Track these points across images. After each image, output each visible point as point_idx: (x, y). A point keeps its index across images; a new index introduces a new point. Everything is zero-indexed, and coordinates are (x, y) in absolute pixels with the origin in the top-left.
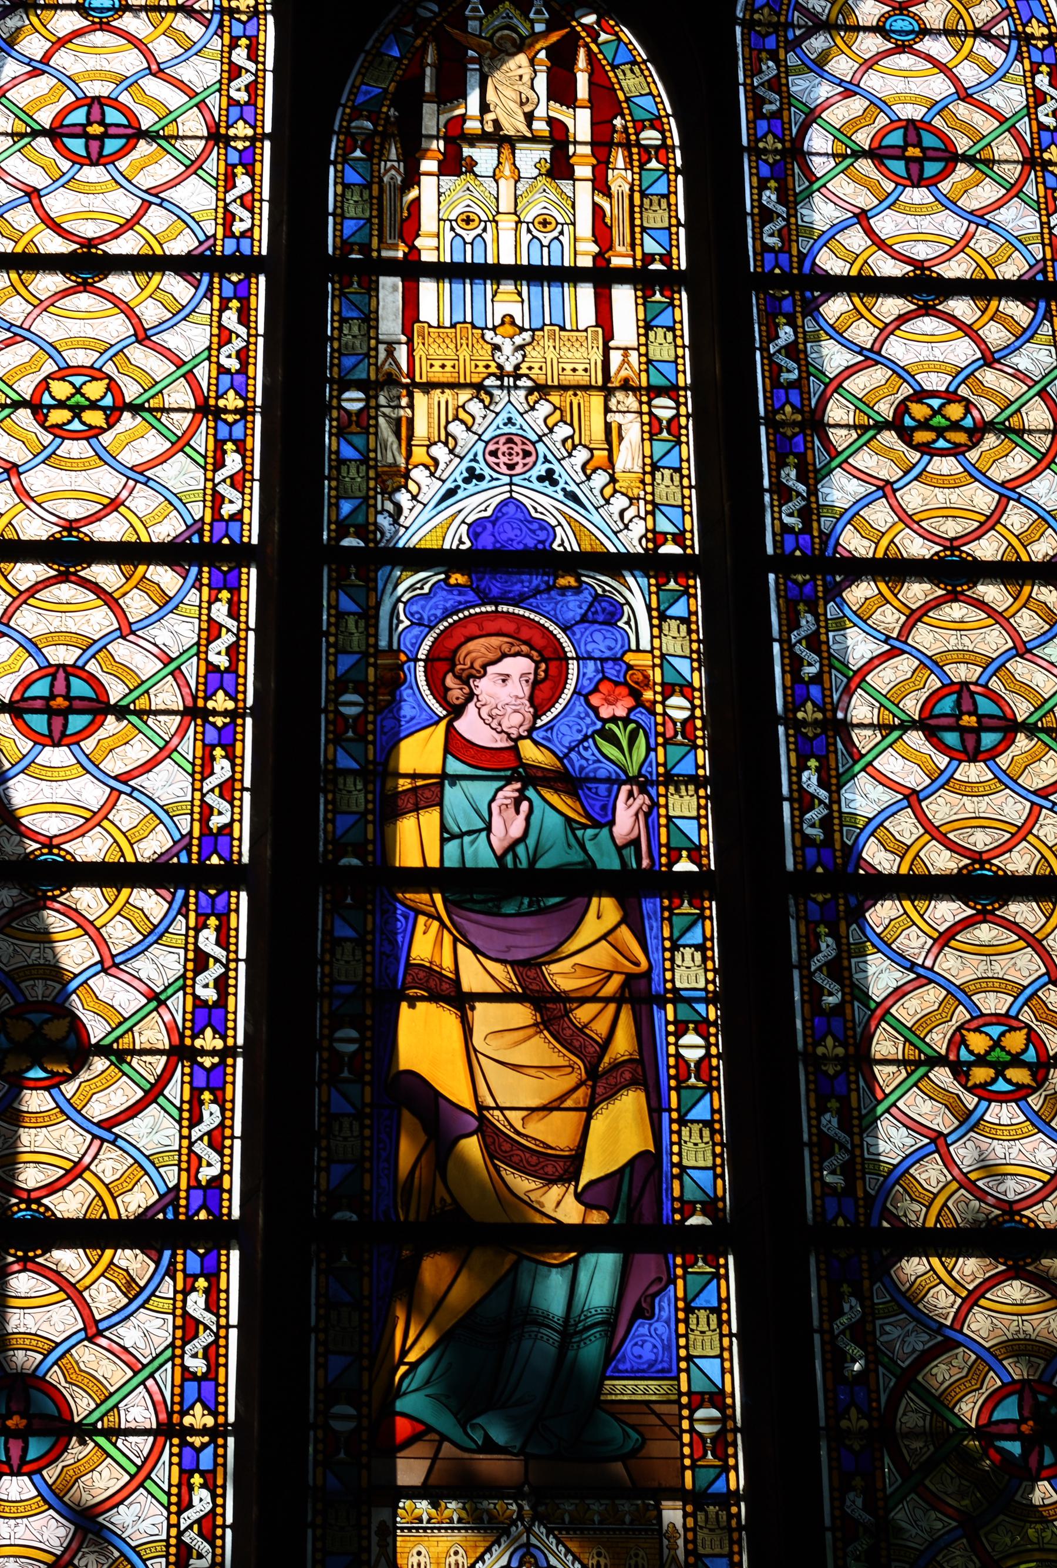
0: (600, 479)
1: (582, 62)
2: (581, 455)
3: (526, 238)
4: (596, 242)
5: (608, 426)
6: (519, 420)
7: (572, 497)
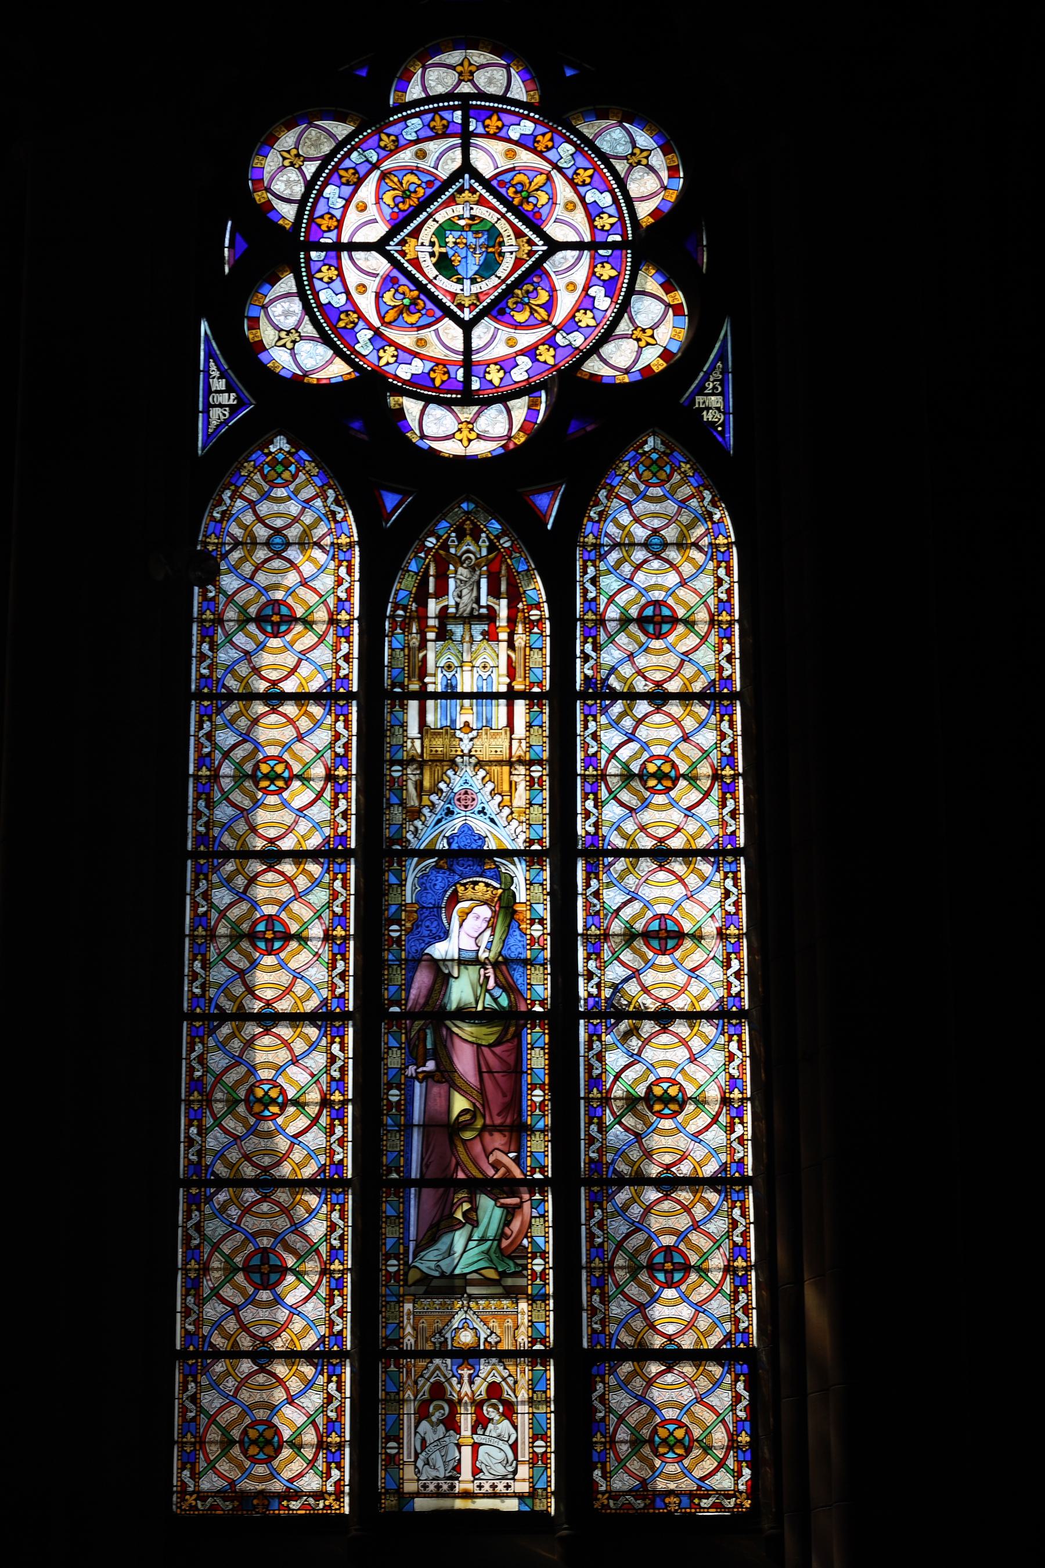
0: (506, 811)
1: (503, 572)
2: (498, 798)
3: (476, 675)
4: (508, 676)
5: (511, 783)
6: (470, 782)
7: (492, 820)
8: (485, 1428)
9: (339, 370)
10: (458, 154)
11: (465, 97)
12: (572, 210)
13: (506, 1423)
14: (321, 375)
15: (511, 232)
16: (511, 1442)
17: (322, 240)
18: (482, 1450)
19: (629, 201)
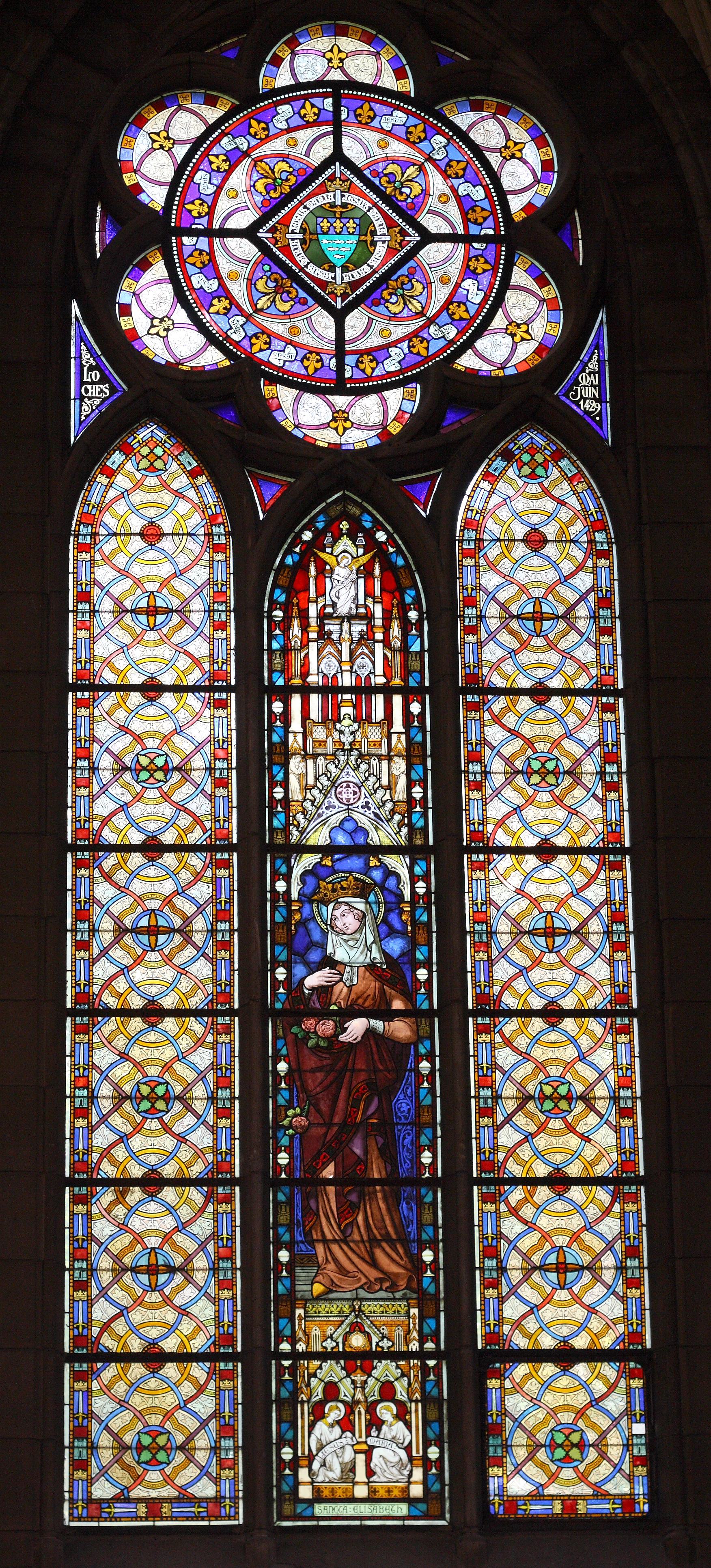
8: (379, 1430)
9: (213, 357)
10: (329, 141)
11: (336, 85)
12: (445, 202)
13: (401, 1424)
14: (196, 363)
15: (382, 221)
16: (406, 1443)
17: (194, 226)
18: (376, 1452)
19: (502, 195)
